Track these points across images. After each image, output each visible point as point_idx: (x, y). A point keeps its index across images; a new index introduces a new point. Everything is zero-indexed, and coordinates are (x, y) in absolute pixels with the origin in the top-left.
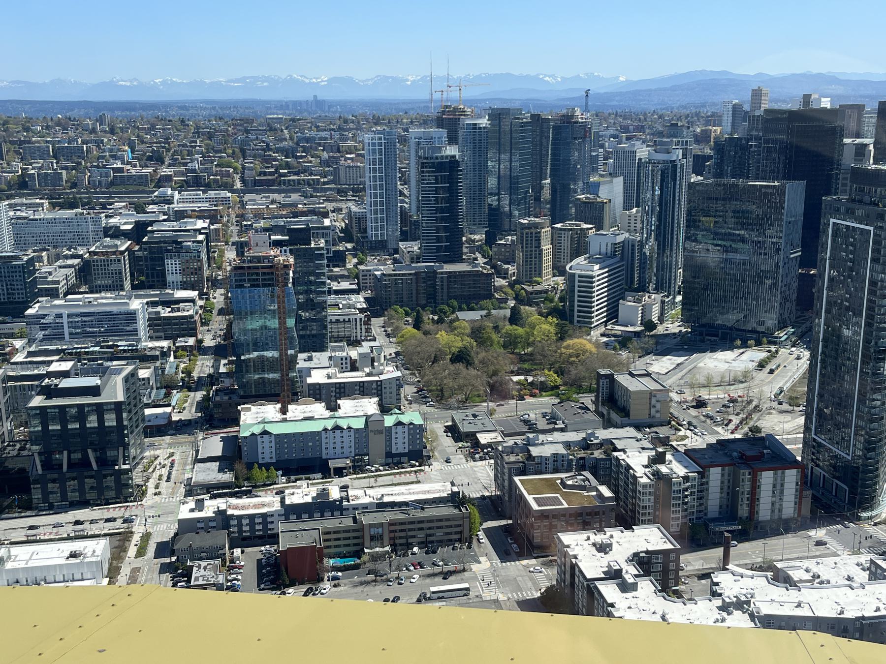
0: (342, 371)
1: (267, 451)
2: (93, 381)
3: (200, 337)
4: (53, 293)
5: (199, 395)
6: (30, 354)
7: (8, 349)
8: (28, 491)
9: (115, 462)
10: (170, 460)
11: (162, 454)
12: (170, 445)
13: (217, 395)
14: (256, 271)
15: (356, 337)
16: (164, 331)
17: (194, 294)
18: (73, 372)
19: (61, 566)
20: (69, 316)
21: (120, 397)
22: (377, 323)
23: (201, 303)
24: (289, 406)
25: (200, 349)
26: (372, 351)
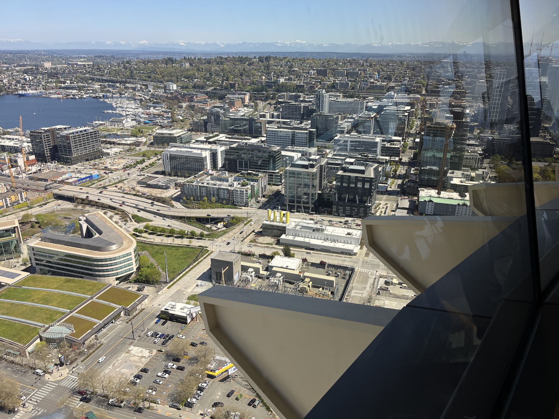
0: (468, 180)
1: (430, 209)
2: (362, 168)
3: (400, 157)
4: (342, 132)
5: (400, 182)
6: (334, 155)
7: (324, 153)
8: (332, 208)
9: (366, 202)
10: (386, 206)
11: (383, 203)
12: (386, 200)
13: (408, 182)
14: (437, 129)
15: (475, 166)
16: (386, 153)
17: (400, 138)
18: (354, 163)
19: (344, 237)
20: (351, 141)
21: (372, 176)
22: (487, 161)
23: (402, 143)
24: (442, 192)
25: (400, 162)
26: (483, 173)
